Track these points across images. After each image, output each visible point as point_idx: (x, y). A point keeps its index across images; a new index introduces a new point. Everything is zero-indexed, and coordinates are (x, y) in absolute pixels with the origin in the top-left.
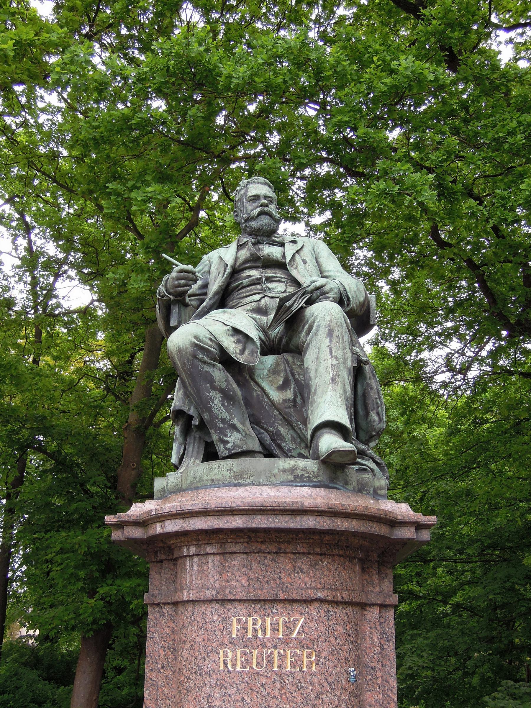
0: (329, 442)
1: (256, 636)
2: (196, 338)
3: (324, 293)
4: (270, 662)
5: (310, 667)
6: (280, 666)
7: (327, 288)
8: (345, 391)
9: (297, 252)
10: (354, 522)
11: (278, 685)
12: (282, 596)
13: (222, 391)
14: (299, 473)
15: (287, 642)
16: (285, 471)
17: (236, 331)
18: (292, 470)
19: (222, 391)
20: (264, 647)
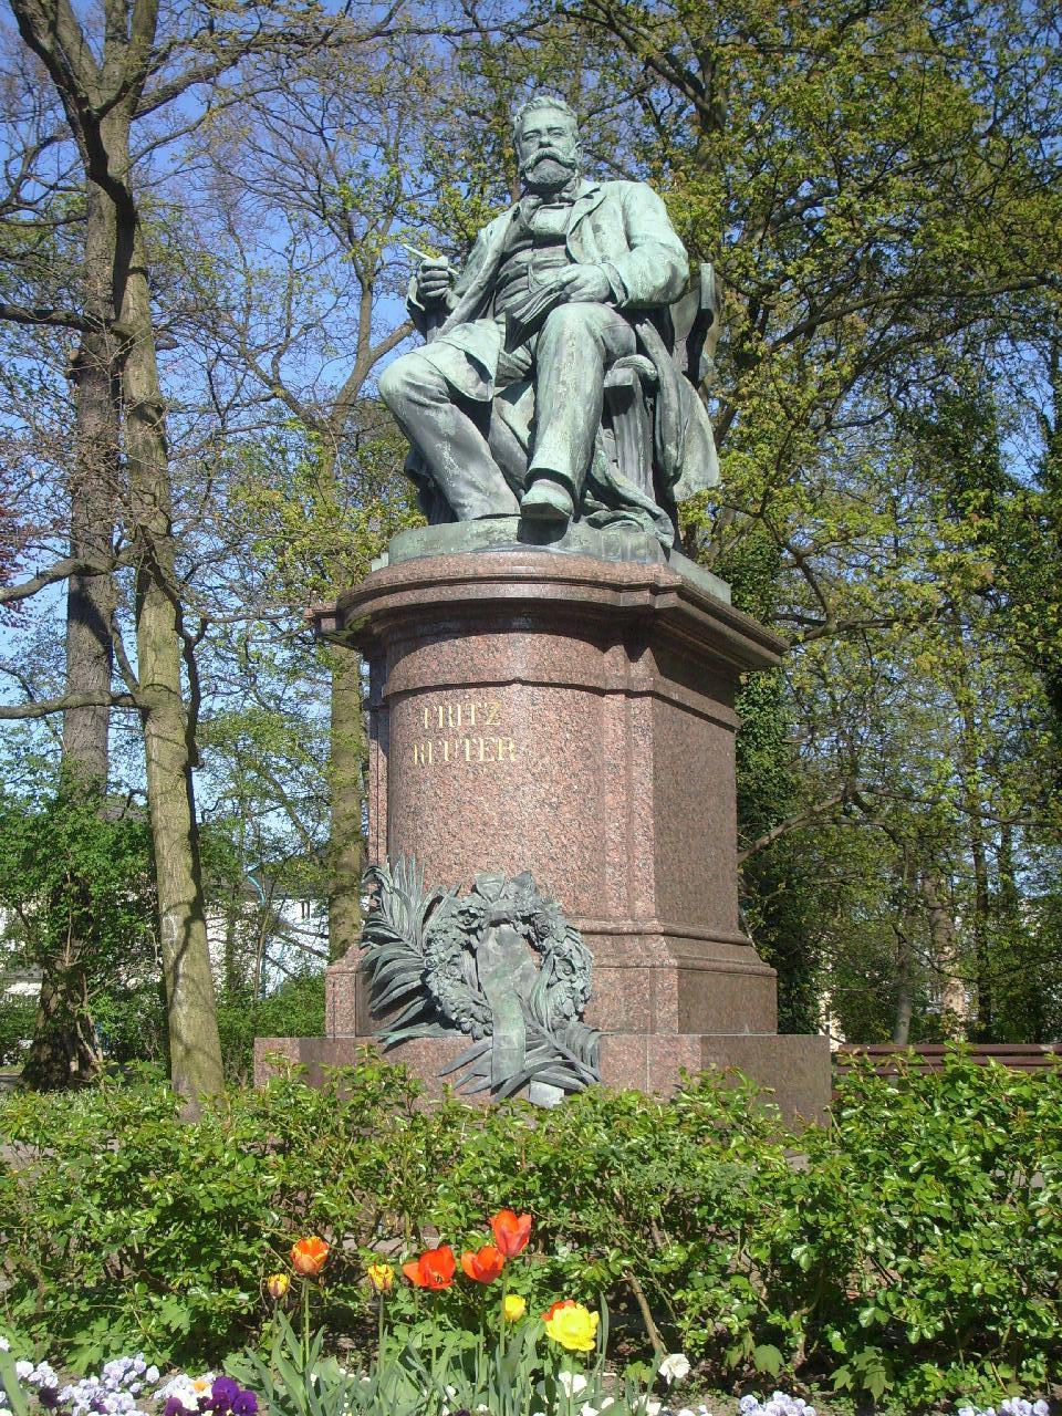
0: (542, 493)
1: (446, 726)
2: (409, 374)
3: (577, 289)
4: (463, 752)
5: (507, 755)
6: (472, 757)
7: (578, 283)
8: (575, 426)
9: (590, 213)
10: (548, 587)
11: (471, 776)
12: (473, 680)
13: (450, 439)
14: (496, 536)
15: (480, 729)
16: (478, 535)
17: (470, 359)
18: (488, 533)
19: (450, 439)
20: (456, 736)
